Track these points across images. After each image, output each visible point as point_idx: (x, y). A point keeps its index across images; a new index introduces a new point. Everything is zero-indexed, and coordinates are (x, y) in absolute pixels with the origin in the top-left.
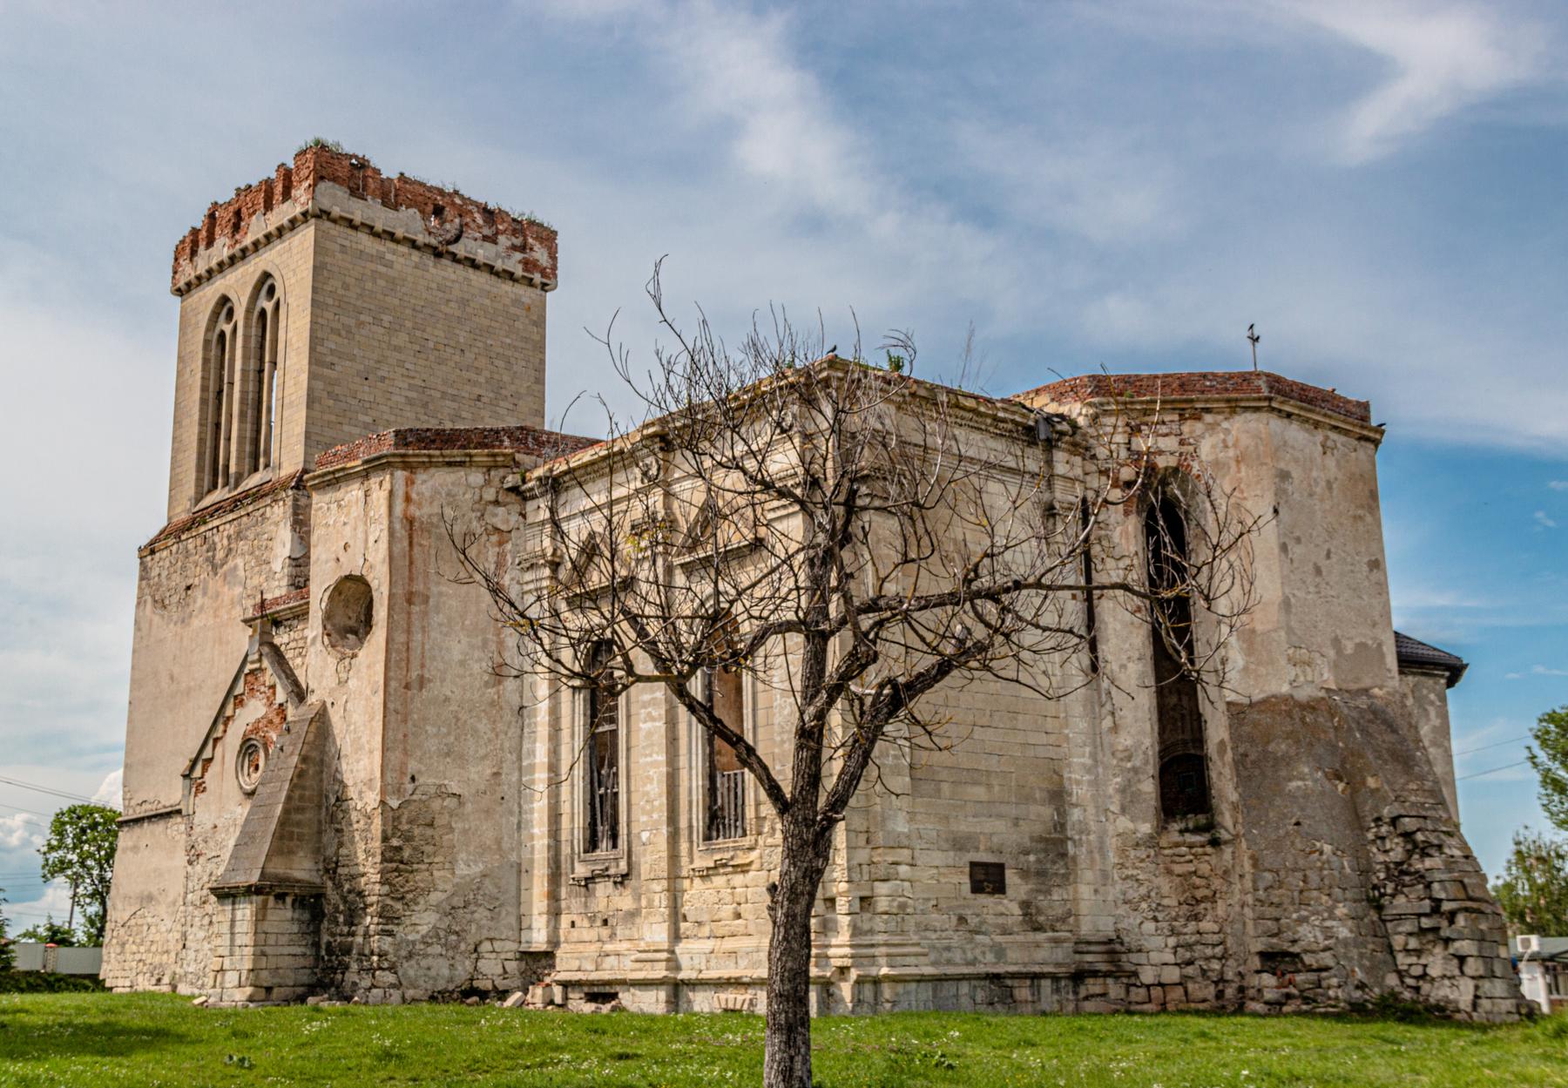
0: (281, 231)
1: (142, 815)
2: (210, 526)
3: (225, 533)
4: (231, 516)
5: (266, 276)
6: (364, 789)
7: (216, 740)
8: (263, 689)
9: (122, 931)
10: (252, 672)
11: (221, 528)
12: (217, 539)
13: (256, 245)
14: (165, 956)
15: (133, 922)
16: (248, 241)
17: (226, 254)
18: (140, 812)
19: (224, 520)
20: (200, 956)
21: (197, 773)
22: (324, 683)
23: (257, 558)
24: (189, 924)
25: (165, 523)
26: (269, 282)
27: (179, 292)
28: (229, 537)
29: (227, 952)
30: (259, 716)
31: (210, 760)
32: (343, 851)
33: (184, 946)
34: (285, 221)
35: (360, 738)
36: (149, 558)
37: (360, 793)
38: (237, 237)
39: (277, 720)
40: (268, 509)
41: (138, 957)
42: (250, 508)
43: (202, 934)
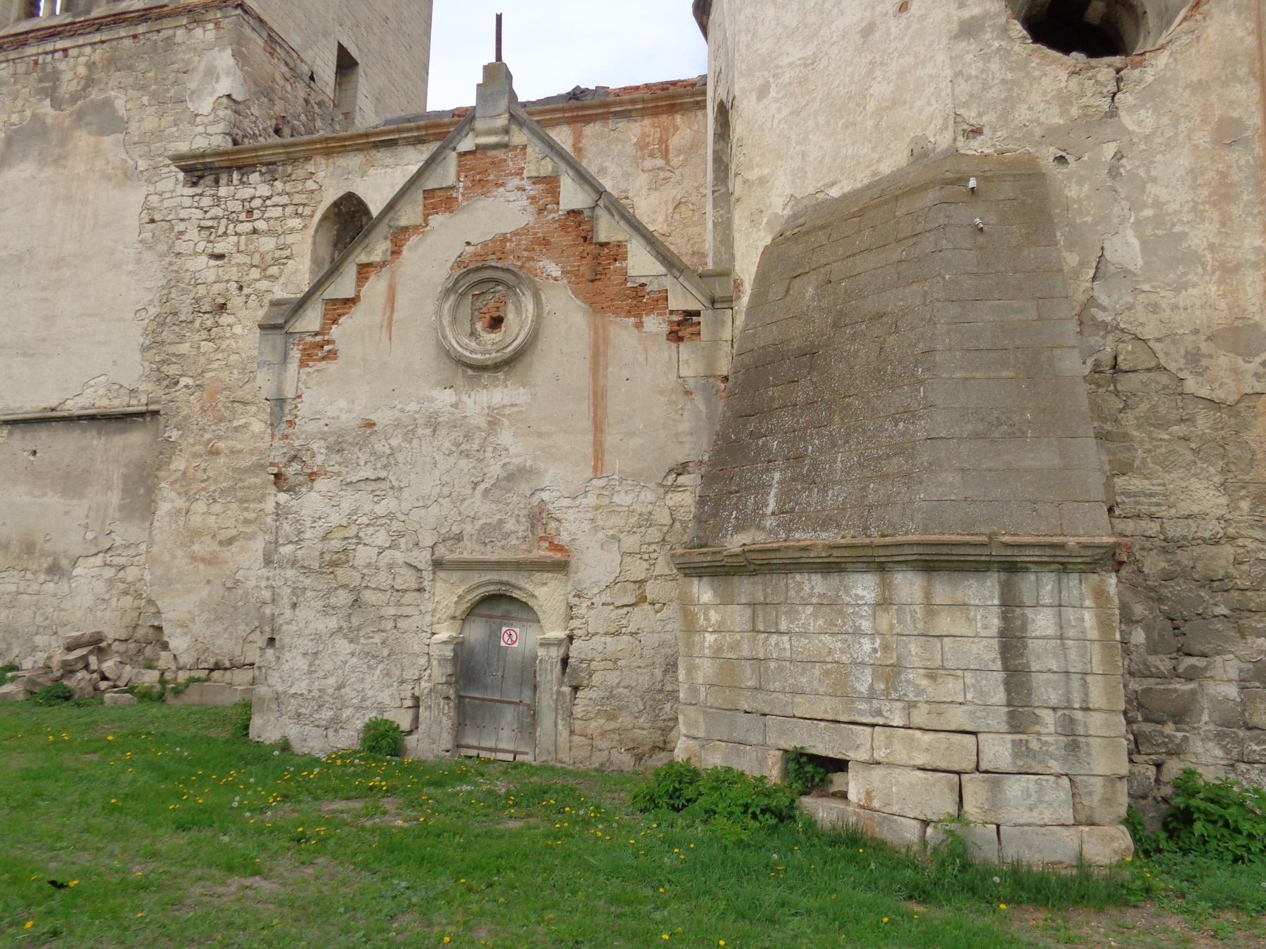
2: (49, 47)
3: (82, 60)
4: (97, 37)
6: (1205, 348)
7: (364, 271)
8: (514, 182)
10: (479, 147)
11: (72, 52)
12: (62, 66)
19: (81, 41)
20: (327, 664)
21: (311, 320)
22: (1022, 114)
23: (154, 95)
24: (286, 602)
28: (91, 66)
29: (998, 719)
30: (507, 228)
31: (350, 302)
32: (1136, 483)
33: (271, 641)
35: (1184, 235)
37: (1194, 358)
39: (567, 240)
40: (180, 32)
43: (333, 623)
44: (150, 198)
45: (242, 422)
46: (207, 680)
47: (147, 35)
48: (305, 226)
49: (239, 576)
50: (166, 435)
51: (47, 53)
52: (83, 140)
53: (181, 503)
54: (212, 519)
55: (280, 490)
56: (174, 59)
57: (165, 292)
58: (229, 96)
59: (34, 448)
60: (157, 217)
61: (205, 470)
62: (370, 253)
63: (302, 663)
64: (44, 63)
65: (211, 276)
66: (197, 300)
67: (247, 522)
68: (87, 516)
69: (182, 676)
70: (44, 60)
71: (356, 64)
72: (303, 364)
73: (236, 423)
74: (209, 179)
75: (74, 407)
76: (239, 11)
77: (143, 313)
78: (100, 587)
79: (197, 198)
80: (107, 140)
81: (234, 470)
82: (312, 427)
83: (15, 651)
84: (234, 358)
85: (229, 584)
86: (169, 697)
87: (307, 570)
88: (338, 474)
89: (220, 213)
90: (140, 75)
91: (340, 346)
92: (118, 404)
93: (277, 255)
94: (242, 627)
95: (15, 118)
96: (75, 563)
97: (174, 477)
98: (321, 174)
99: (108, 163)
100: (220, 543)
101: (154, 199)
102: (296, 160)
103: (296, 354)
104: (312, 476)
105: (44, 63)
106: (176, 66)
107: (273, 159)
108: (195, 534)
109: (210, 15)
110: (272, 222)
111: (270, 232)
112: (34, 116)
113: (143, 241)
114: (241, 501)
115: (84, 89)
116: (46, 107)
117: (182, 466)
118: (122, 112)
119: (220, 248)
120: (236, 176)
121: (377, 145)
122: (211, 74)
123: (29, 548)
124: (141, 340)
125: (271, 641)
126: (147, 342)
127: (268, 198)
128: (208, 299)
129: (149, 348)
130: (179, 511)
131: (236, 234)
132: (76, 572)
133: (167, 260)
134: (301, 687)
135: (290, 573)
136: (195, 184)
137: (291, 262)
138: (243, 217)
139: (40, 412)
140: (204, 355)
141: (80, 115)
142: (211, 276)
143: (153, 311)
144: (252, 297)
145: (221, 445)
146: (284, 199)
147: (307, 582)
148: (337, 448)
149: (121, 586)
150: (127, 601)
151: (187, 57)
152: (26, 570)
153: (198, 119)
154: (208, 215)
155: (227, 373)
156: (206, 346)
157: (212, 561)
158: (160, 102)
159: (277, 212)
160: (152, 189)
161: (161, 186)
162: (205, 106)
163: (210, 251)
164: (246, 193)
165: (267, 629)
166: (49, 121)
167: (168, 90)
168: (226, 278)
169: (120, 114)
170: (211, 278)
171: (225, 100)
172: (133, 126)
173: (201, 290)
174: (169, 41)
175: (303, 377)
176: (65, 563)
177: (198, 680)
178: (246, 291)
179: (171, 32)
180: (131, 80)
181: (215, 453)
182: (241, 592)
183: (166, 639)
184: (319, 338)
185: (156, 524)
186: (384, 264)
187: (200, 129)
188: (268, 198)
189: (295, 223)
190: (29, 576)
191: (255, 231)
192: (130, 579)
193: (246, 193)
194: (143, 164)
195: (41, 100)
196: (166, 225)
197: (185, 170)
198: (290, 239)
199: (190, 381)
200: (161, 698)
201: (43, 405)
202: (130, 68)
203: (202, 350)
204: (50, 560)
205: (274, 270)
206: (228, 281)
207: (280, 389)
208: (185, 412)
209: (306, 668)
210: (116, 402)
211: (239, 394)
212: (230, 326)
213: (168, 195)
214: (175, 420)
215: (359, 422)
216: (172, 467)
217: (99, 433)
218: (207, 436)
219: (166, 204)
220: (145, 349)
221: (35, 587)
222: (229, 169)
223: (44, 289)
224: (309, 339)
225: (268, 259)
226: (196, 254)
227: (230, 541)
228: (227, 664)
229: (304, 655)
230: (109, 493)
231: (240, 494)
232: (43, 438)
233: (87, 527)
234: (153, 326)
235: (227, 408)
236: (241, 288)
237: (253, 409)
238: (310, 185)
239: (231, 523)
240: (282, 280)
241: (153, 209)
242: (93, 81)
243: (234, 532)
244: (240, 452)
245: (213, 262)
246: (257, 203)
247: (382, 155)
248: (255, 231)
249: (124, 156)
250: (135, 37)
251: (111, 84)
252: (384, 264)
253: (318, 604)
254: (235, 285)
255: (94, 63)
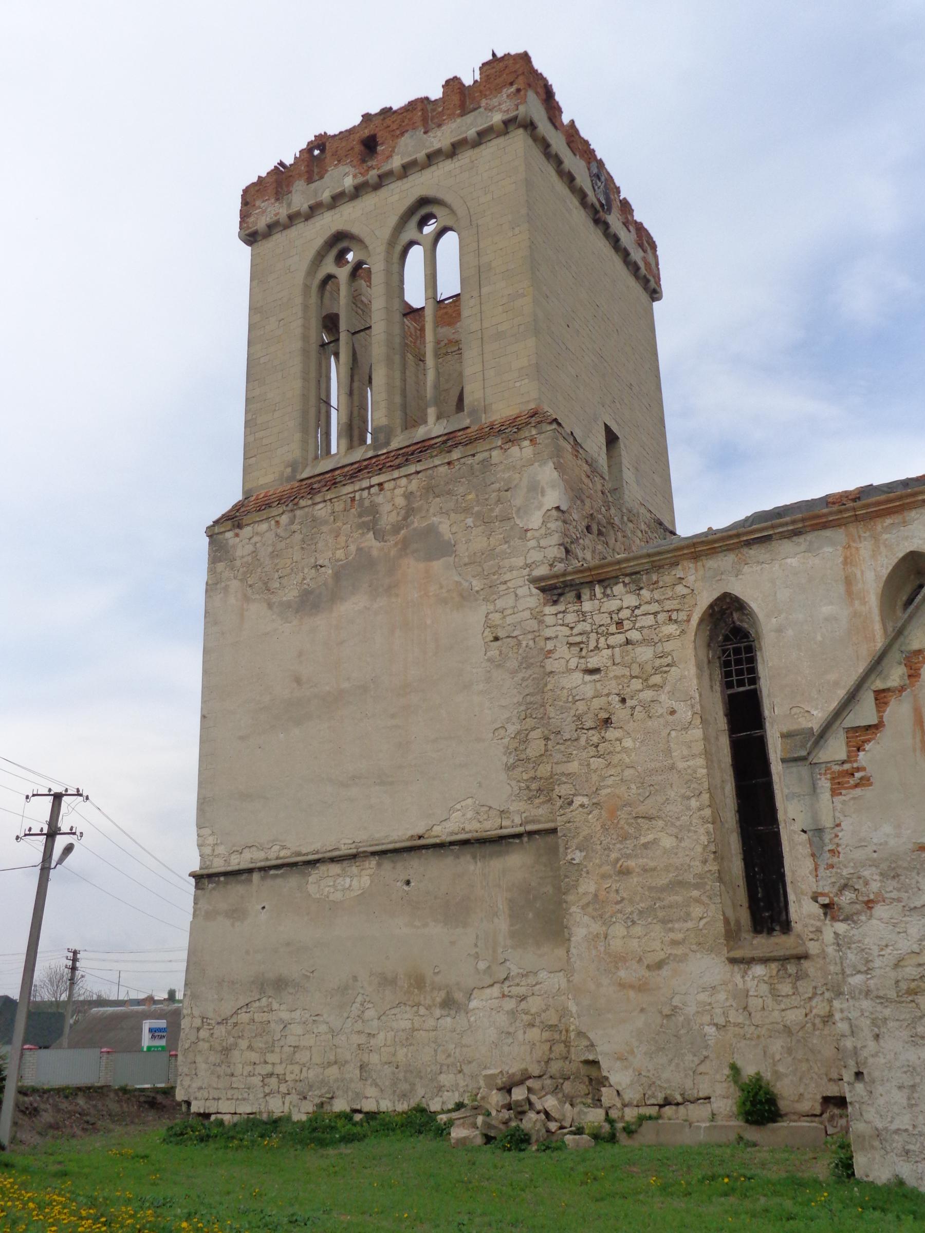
0: (455, 149)
1: (244, 865)
2: (365, 484)
3: (399, 491)
4: (412, 469)
5: (424, 201)
7: (882, 697)
9: (220, 1031)
11: (386, 486)
12: (380, 499)
13: (407, 169)
14: (333, 1071)
15: (244, 1017)
16: (396, 162)
17: (349, 182)
18: (236, 863)
25: (239, 497)
26: (424, 211)
27: (251, 237)
28: (408, 496)
34: (471, 133)
36: (229, 535)
38: (373, 163)
40: (495, 453)
41: (268, 1069)
42: (456, 454)
44: (490, 616)
45: (650, 837)
46: (659, 1117)
47: (462, 461)
48: (683, 632)
49: (676, 1002)
50: (569, 857)
51: (363, 490)
52: (412, 567)
53: (596, 927)
54: (634, 943)
55: (834, 919)
56: (493, 480)
57: (523, 708)
58: (558, 508)
59: (407, 878)
60: (501, 634)
61: (617, 891)
62: (885, 679)
63: (900, 1098)
64: (361, 499)
65: (589, 691)
66: (579, 718)
67: (674, 943)
68: (476, 945)
69: (630, 1114)
70: (361, 496)
71: (617, 438)
72: (834, 792)
73: (643, 840)
74: (571, 596)
75: (443, 832)
76: (554, 426)
77: (502, 732)
78: (502, 1020)
79: (560, 616)
80: (437, 565)
81: (651, 888)
82: (859, 854)
83: (421, 1091)
84: (628, 773)
85: (666, 1011)
86: (622, 1137)
87: (883, 1000)
88: (899, 900)
89: (588, 628)
90: (460, 499)
91: (870, 770)
92: (490, 826)
93: (658, 662)
94: (689, 1057)
95: (340, 554)
96: (469, 996)
97: (585, 901)
98: (691, 579)
99: (441, 587)
100: (648, 967)
101: (496, 618)
102: (661, 567)
103: (825, 784)
104: (869, 904)
105: (361, 499)
106: (496, 486)
107: (637, 569)
108: (619, 959)
109: (525, 433)
110: (645, 631)
111: (645, 641)
112: (359, 550)
113: (490, 660)
114: (664, 922)
115: (405, 518)
116: (369, 540)
117: (592, 888)
118: (447, 536)
119: (593, 662)
120: (598, 590)
121: (749, 544)
122: (535, 488)
123: (419, 982)
124: (505, 759)
125: (859, 1075)
126: (511, 761)
127: (637, 607)
128: (591, 715)
129: (513, 767)
130: (597, 936)
131: (609, 647)
132: (473, 1004)
133: (520, 675)
134: (903, 1121)
135: (866, 1004)
136: (555, 602)
137: (673, 669)
138: (613, 629)
139: (408, 840)
140: (595, 771)
141: (405, 545)
142: (589, 691)
143: (512, 729)
144: (638, 709)
145: (631, 863)
146: (655, 607)
147: (887, 1012)
148: (892, 873)
149: (526, 1018)
150: (535, 1034)
151: (506, 475)
152: (418, 1005)
153: (529, 534)
154: (575, 631)
155: (623, 788)
156: (596, 763)
157: (642, 987)
158: (485, 521)
159: (649, 621)
160: (491, 607)
161: (500, 604)
162: (535, 520)
163: (583, 667)
164: (613, 604)
165: (851, 1063)
166: (375, 553)
167: (492, 510)
168: (606, 691)
169: (446, 538)
170: (590, 694)
171: (554, 513)
172: (461, 548)
173: (581, 707)
174: (486, 464)
175: (839, 806)
176: (459, 996)
177: (650, 1118)
178: (629, 703)
179: (486, 454)
180: (451, 505)
181: (625, 872)
182: (681, 1019)
183: (605, 1074)
184: (847, 766)
185: (573, 951)
186: (902, 689)
187: (533, 543)
188: (637, 607)
189: (671, 629)
190: (422, 1011)
191: (628, 642)
192: (533, 1011)
193: (613, 604)
194: (477, 584)
195: (363, 534)
196: (513, 642)
197: (543, 590)
198: (668, 646)
199: (585, 800)
200: (612, 1138)
201: (410, 833)
202: (449, 493)
203: (593, 767)
204: (443, 994)
205: (656, 679)
206: (608, 695)
207: (815, 817)
208: (585, 832)
209: (905, 1102)
210: (488, 825)
211: (642, 809)
212: (619, 740)
213: (509, 611)
214: (576, 841)
215: (910, 846)
216: (581, 890)
217: (474, 857)
218: (614, 855)
219: (509, 620)
220: (510, 768)
221: (431, 1023)
222: (590, 584)
223: (393, 716)
224: (836, 768)
225: (649, 668)
226: (569, 671)
227: (659, 965)
228: (679, 1099)
229: (900, 1088)
230: (496, 920)
231: (661, 914)
232: (414, 866)
233: (477, 956)
234: (515, 744)
235: (630, 825)
236: (623, 701)
237: (660, 823)
238: (680, 590)
239: (657, 945)
240: (667, 688)
241: (496, 626)
242: (413, 509)
243: (662, 955)
244: (654, 869)
245: (588, 678)
246: (625, 614)
247: (754, 552)
248: (628, 642)
249: (457, 578)
250: (449, 463)
251: (431, 511)
252: (902, 689)
253: (905, 1034)
254: (617, 698)
255: (411, 493)
